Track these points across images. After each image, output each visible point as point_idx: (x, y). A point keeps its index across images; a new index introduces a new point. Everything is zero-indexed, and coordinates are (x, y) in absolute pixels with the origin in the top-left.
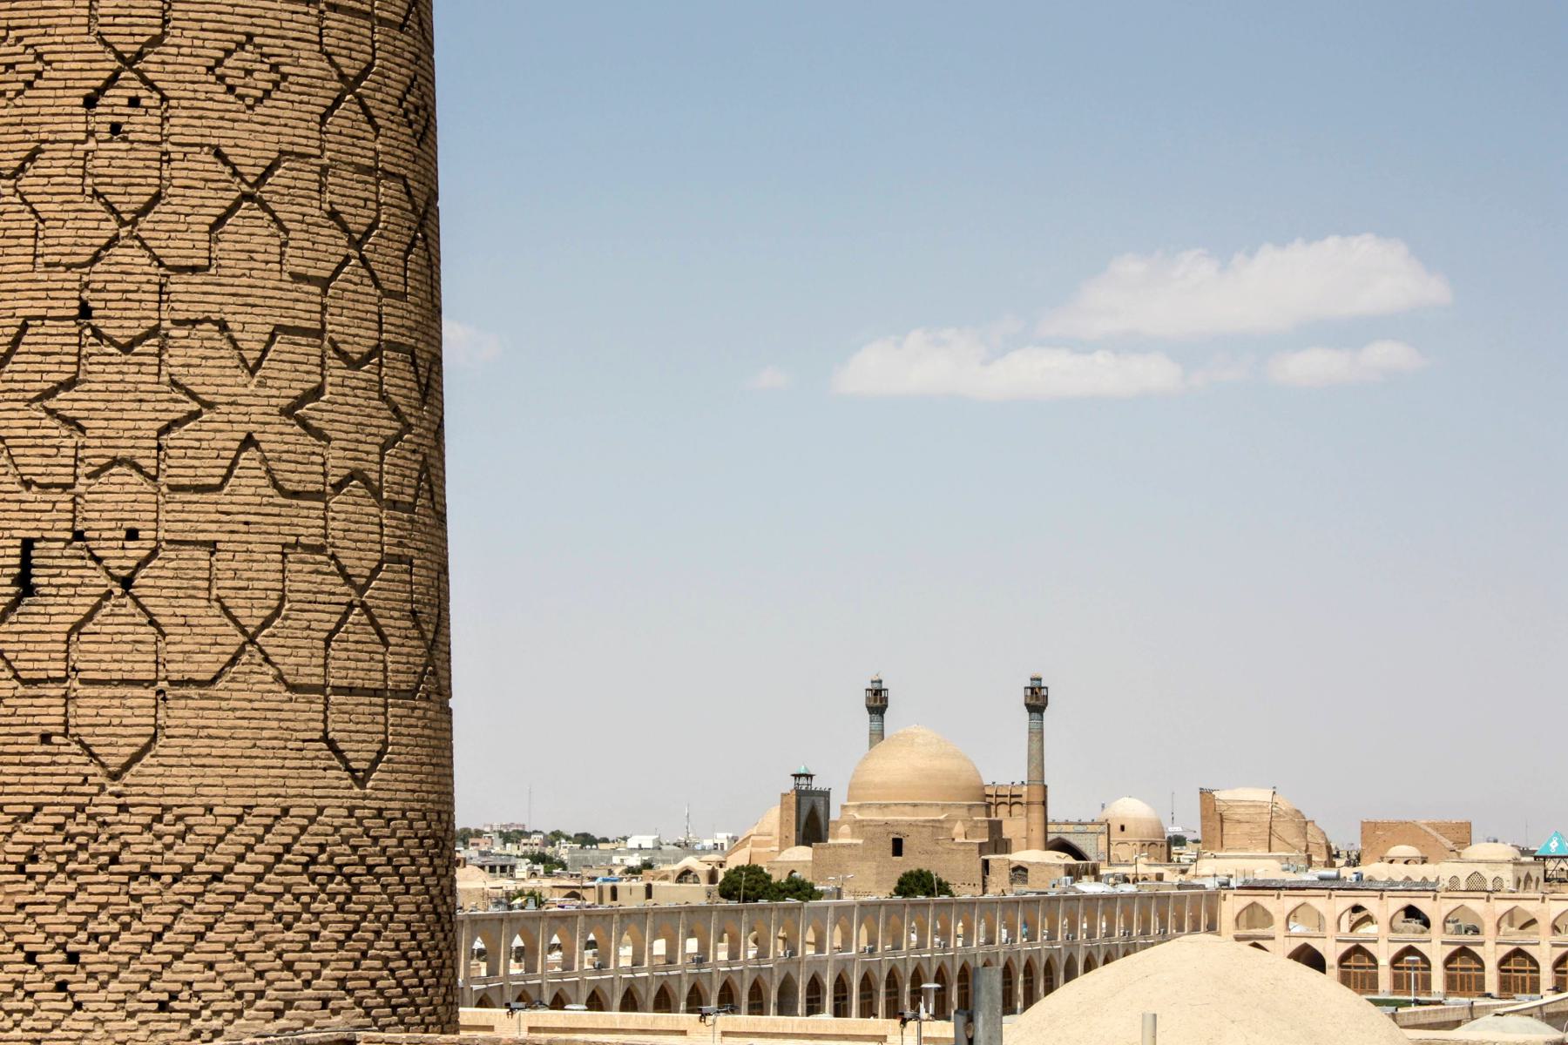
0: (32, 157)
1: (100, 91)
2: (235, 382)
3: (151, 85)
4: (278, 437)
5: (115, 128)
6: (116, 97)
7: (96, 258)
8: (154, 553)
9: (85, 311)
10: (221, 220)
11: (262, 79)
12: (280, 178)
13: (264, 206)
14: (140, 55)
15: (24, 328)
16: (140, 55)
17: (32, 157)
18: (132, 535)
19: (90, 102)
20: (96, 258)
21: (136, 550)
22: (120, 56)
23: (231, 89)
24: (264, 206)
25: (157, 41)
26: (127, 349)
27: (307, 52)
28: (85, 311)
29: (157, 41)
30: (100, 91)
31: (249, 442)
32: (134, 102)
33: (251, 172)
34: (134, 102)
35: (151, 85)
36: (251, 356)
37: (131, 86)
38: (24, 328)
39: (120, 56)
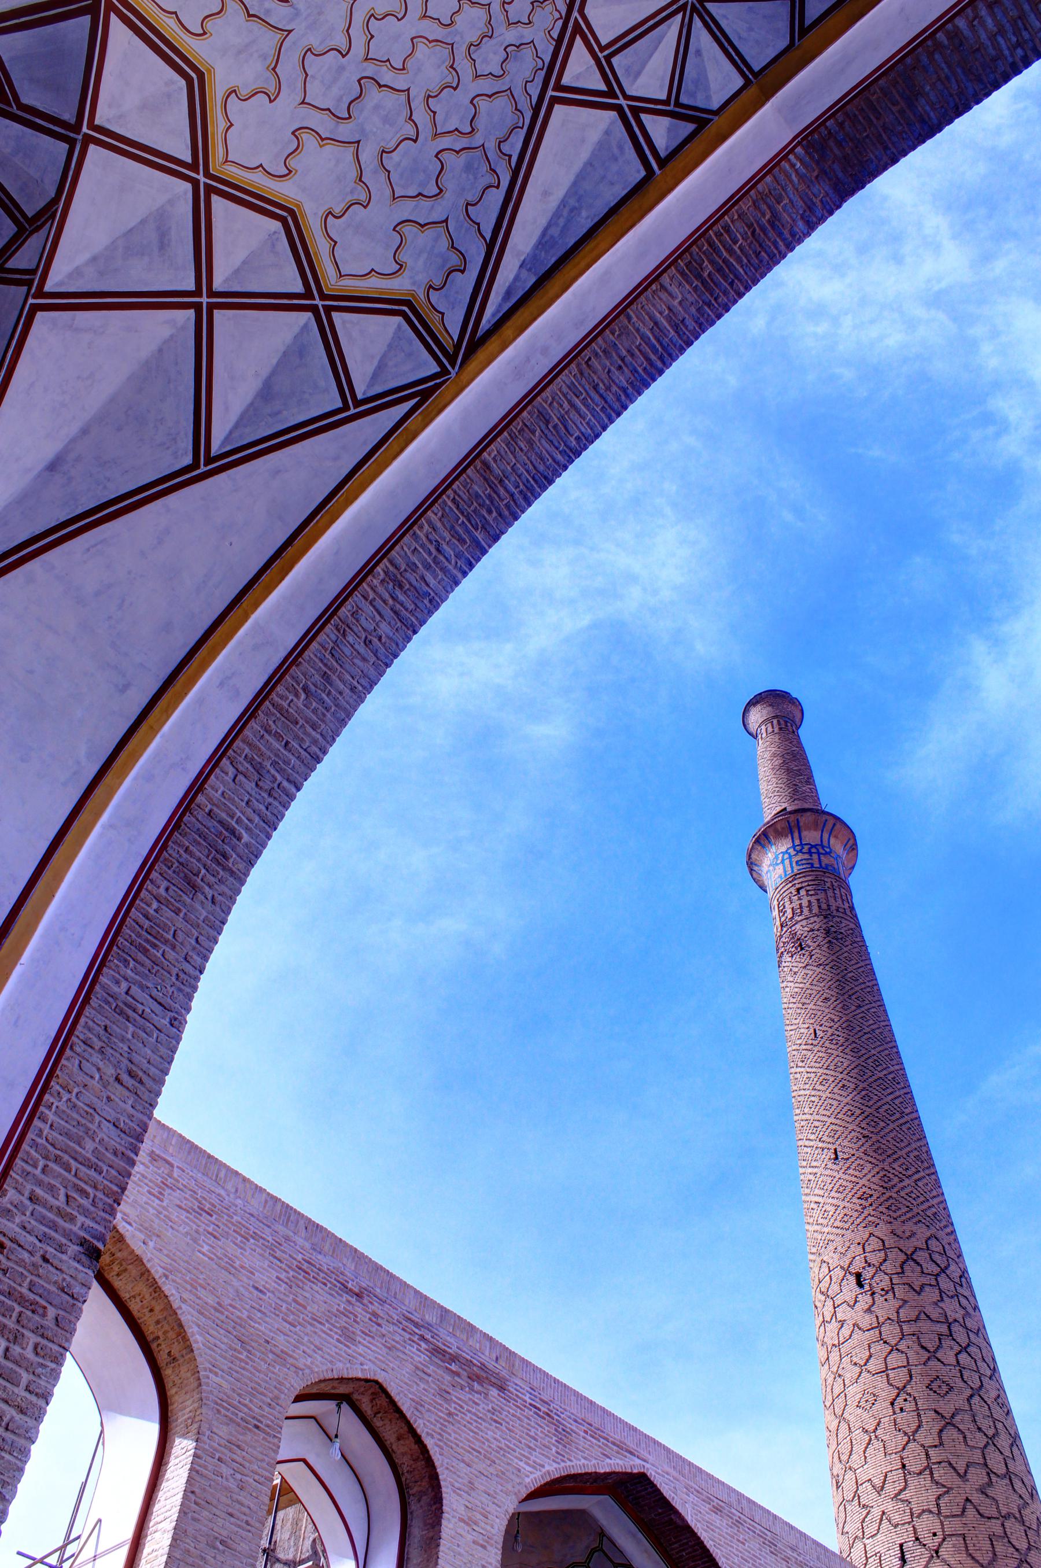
0: (878, 1424)
1: (895, 1400)
2: (957, 1481)
3: (910, 1395)
4: (976, 1497)
5: (901, 1409)
6: (900, 1400)
7: (904, 1449)
8: (944, 1540)
9: (904, 1466)
10: (941, 1431)
11: (945, 1388)
12: (958, 1418)
13: (954, 1425)
14: (904, 1387)
15: (886, 1476)
16: (904, 1387)
17: (878, 1424)
18: (935, 1534)
19: (892, 1404)
20: (904, 1449)
21: (938, 1539)
22: (898, 1388)
23: (935, 1392)
24: (954, 1425)
25: (909, 1382)
26: (920, 1473)
27: (958, 1380)
28: (904, 1466)
29: (909, 1382)
30: (895, 1400)
31: (967, 1500)
32: (905, 1400)
33: (948, 1416)
34: (905, 1400)
35: (910, 1395)
36: (962, 1472)
37: (903, 1396)
38: (886, 1476)
39: (898, 1388)
